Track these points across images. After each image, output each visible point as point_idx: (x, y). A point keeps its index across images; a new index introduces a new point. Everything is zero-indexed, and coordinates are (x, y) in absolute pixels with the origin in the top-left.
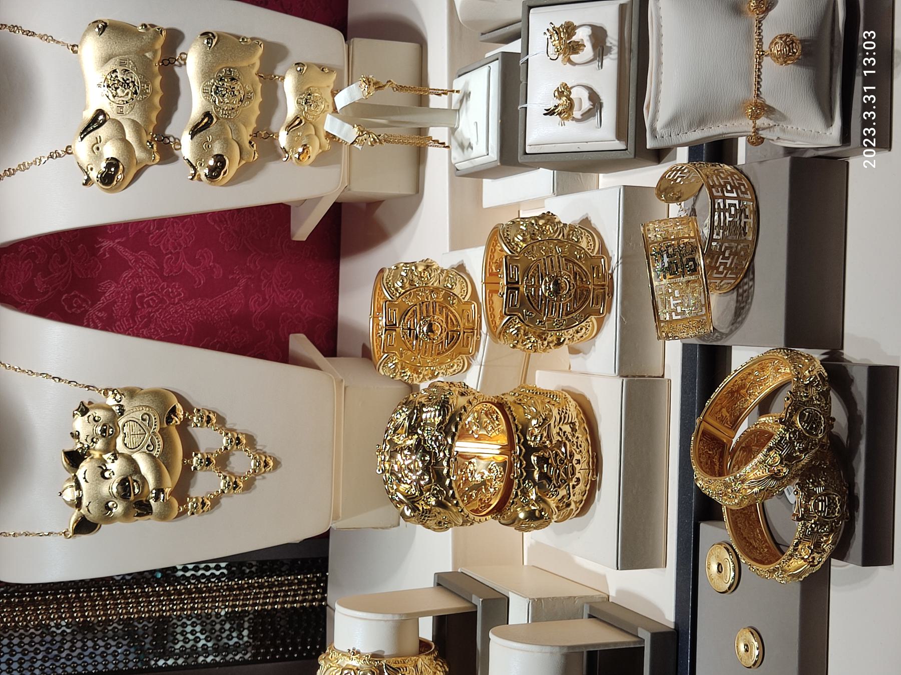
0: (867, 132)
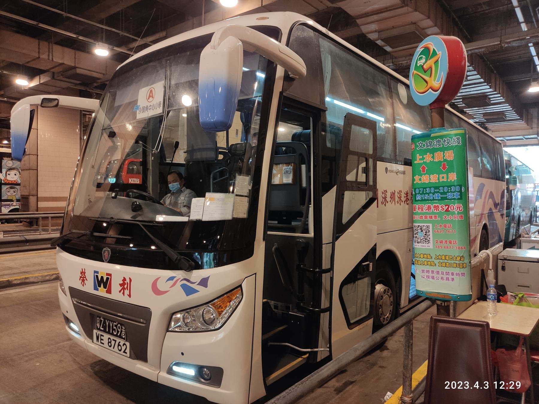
0: (467, 383)
